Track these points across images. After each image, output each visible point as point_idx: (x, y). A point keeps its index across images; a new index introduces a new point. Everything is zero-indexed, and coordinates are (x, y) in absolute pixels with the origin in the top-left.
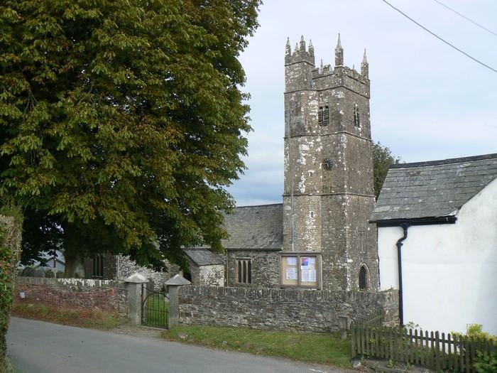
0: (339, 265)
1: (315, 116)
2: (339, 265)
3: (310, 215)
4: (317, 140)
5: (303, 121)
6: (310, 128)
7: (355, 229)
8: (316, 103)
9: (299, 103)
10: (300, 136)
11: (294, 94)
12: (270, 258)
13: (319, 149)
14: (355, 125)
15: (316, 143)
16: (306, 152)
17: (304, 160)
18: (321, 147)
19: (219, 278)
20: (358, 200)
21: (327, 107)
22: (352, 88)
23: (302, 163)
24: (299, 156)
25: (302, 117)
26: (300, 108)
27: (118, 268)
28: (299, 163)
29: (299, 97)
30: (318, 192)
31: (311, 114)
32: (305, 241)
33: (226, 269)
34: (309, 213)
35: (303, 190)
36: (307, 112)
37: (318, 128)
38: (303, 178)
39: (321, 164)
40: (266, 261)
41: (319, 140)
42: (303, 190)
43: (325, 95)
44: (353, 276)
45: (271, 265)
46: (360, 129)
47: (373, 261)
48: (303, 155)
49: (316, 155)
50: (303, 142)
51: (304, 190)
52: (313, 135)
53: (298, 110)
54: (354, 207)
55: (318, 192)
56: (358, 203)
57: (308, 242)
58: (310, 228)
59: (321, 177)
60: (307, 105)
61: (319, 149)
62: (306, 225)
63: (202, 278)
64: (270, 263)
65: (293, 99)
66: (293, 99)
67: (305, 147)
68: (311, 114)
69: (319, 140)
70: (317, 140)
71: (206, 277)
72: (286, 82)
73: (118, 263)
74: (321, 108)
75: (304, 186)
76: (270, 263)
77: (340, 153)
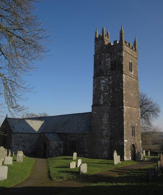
0: (120, 143)
1: (109, 66)
2: (120, 143)
3: (105, 116)
4: (110, 78)
5: (103, 68)
6: (106, 72)
7: (129, 124)
8: (110, 60)
9: (101, 60)
10: (101, 76)
11: (99, 55)
12: (85, 138)
13: (111, 83)
14: (130, 71)
15: (109, 79)
16: (104, 84)
17: (103, 88)
18: (112, 82)
19: (61, 147)
20: (131, 109)
21: (115, 61)
22: (128, 52)
23: (102, 89)
24: (100, 86)
25: (102, 66)
26: (101, 62)
27: (13, 141)
28: (100, 90)
29: (101, 56)
30: (110, 104)
31: (107, 65)
32: (102, 129)
33: (64, 143)
34: (104, 115)
35: (102, 103)
36: (105, 63)
37: (110, 72)
38: (102, 97)
39: (111, 90)
40: (83, 139)
41: (110, 78)
42: (102, 103)
43: (114, 55)
44: (127, 149)
45: (85, 142)
46: (132, 73)
47: (138, 142)
48: (102, 85)
49: (109, 85)
50: (102, 79)
51: (102, 103)
52: (108, 75)
53: (100, 63)
54: (129, 112)
55: (110, 104)
56: (131, 111)
57: (104, 130)
58: (105, 122)
59: (111, 97)
60: (105, 60)
61: (111, 83)
62: (103, 121)
63: (51, 147)
64: (85, 140)
65: (98, 58)
66: (98, 58)
67: (103, 81)
68: (107, 65)
69: (110, 78)
70: (110, 78)
71: (53, 147)
72: (95, 50)
73: (13, 139)
74: (112, 62)
75: (102, 101)
76: (85, 140)
77: (121, 84)
